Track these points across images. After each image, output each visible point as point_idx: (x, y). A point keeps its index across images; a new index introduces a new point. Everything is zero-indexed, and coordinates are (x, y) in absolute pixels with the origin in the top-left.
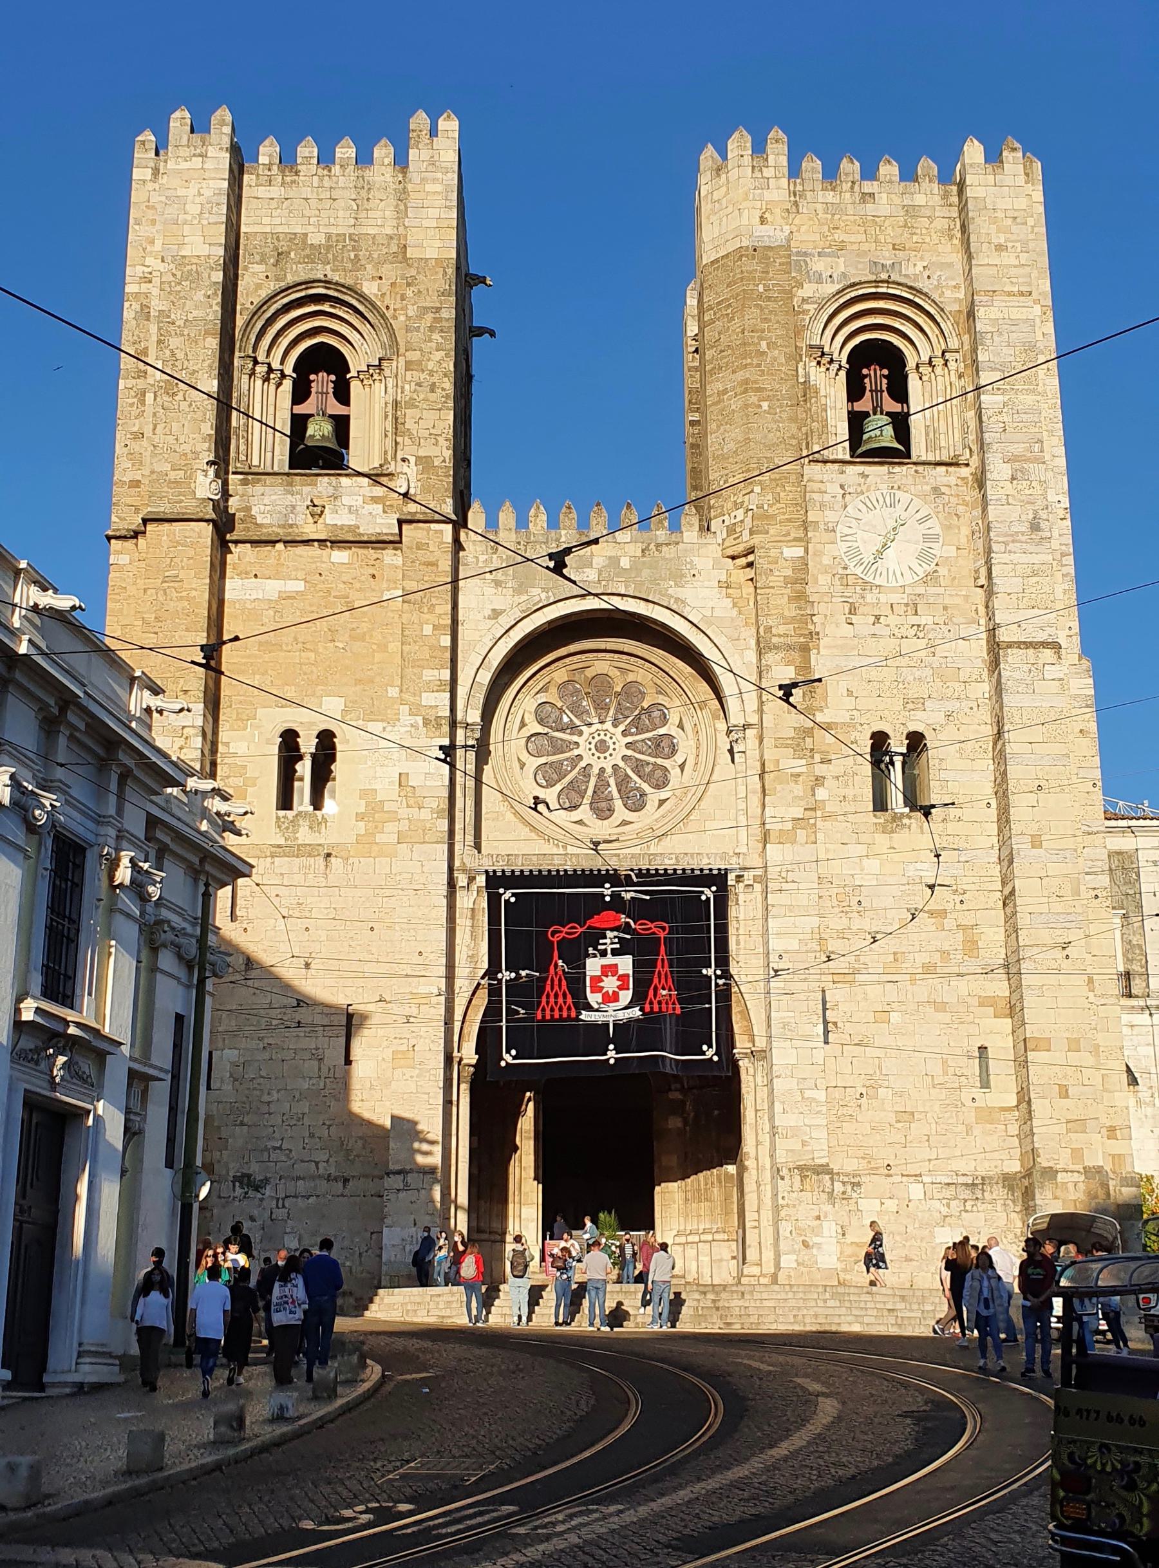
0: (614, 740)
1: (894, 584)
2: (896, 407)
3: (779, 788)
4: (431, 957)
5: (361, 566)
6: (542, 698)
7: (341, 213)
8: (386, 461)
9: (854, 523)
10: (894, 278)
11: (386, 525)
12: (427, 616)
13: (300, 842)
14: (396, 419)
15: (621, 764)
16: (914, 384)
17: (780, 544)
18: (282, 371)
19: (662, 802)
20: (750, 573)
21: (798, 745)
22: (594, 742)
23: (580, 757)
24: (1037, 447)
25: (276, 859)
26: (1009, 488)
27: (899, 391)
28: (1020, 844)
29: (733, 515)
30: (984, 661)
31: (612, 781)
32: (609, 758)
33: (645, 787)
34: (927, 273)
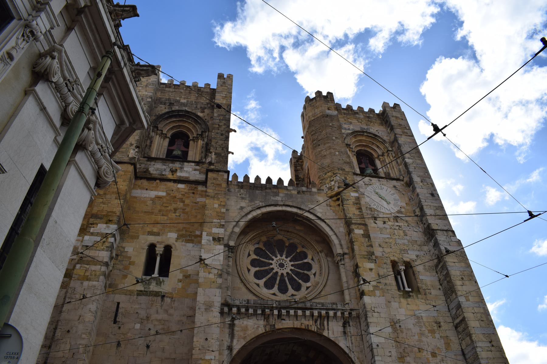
0: (286, 263)
1: (387, 212)
2: (373, 168)
3: (365, 273)
4: (212, 341)
5: (189, 190)
6: (257, 246)
7: (192, 96)
8: (201, 159)
9: (370, 193)
10: (368, 131)
11: (202, 177)
12: (216, 202)
13: (151, 290)
14: (207, 148)
15: (290, 272)
16: (378, 163)
17: (349, 192)
18: (166, 134)
19: (308, 288)
20: (340, 202)
21: (370, 258)
22: (278, 263)
23: (273, 269)
24: (426, 174)
25: (140, 297)
26: (421, 184)
27: (373, 164)
28: (462, 299)
29: (329, 184)
30: (425, 239)
31: (286, 279)
32: (284, 269)
33: (300, 281)
34: (378, 132)
